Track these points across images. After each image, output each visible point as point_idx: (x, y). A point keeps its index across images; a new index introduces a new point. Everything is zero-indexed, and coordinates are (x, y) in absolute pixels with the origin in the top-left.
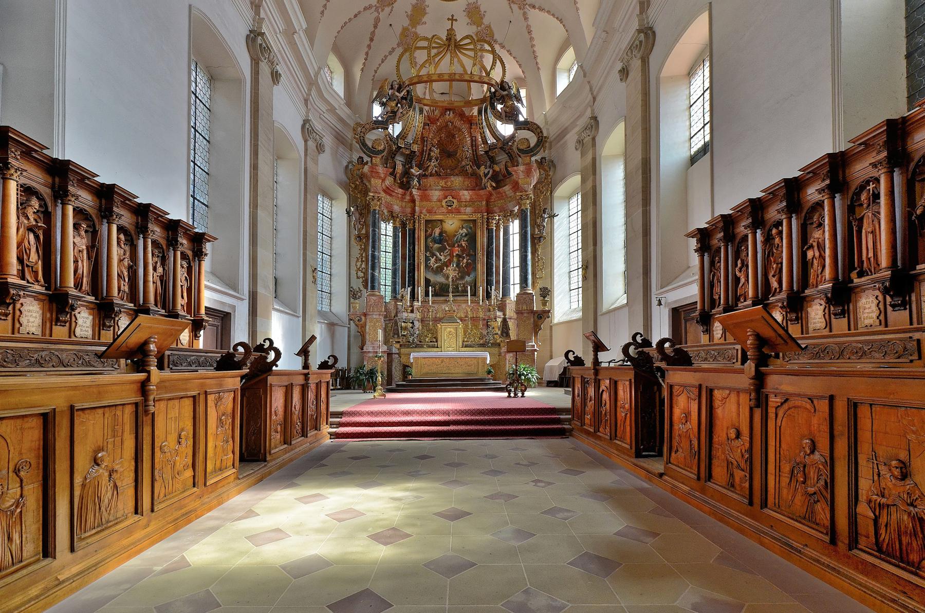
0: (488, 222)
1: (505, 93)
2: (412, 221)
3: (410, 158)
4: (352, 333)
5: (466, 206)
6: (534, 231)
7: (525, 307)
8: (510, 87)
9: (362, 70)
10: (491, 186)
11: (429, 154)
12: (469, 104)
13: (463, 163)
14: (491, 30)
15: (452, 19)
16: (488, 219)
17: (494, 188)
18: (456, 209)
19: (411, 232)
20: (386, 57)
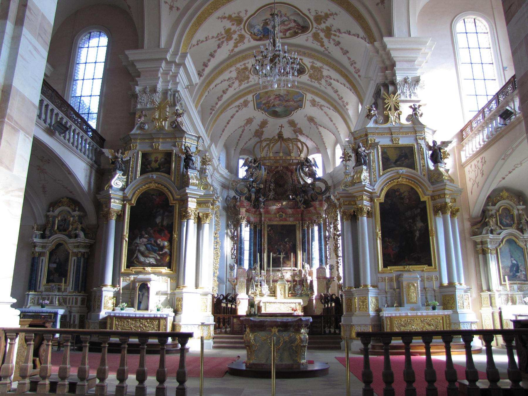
0: (302, 226)
1: (308, 164)
2: (260, 225)
3: (258, 191)
4: (228, 288)
5: (290, 217)
6: (326, 234)
7: (321, 275)
8: (311, 161)
9: (235, 150)
10: (303, 207)
11: (269, 187)
12: (290, 164)
13: (288, 193)
14: (301, 130)
15: (282, 127)
16: (302, 224)
17: (305, 208)
18: (284, 218)
19: (260, 231)
20: (247, 142)
